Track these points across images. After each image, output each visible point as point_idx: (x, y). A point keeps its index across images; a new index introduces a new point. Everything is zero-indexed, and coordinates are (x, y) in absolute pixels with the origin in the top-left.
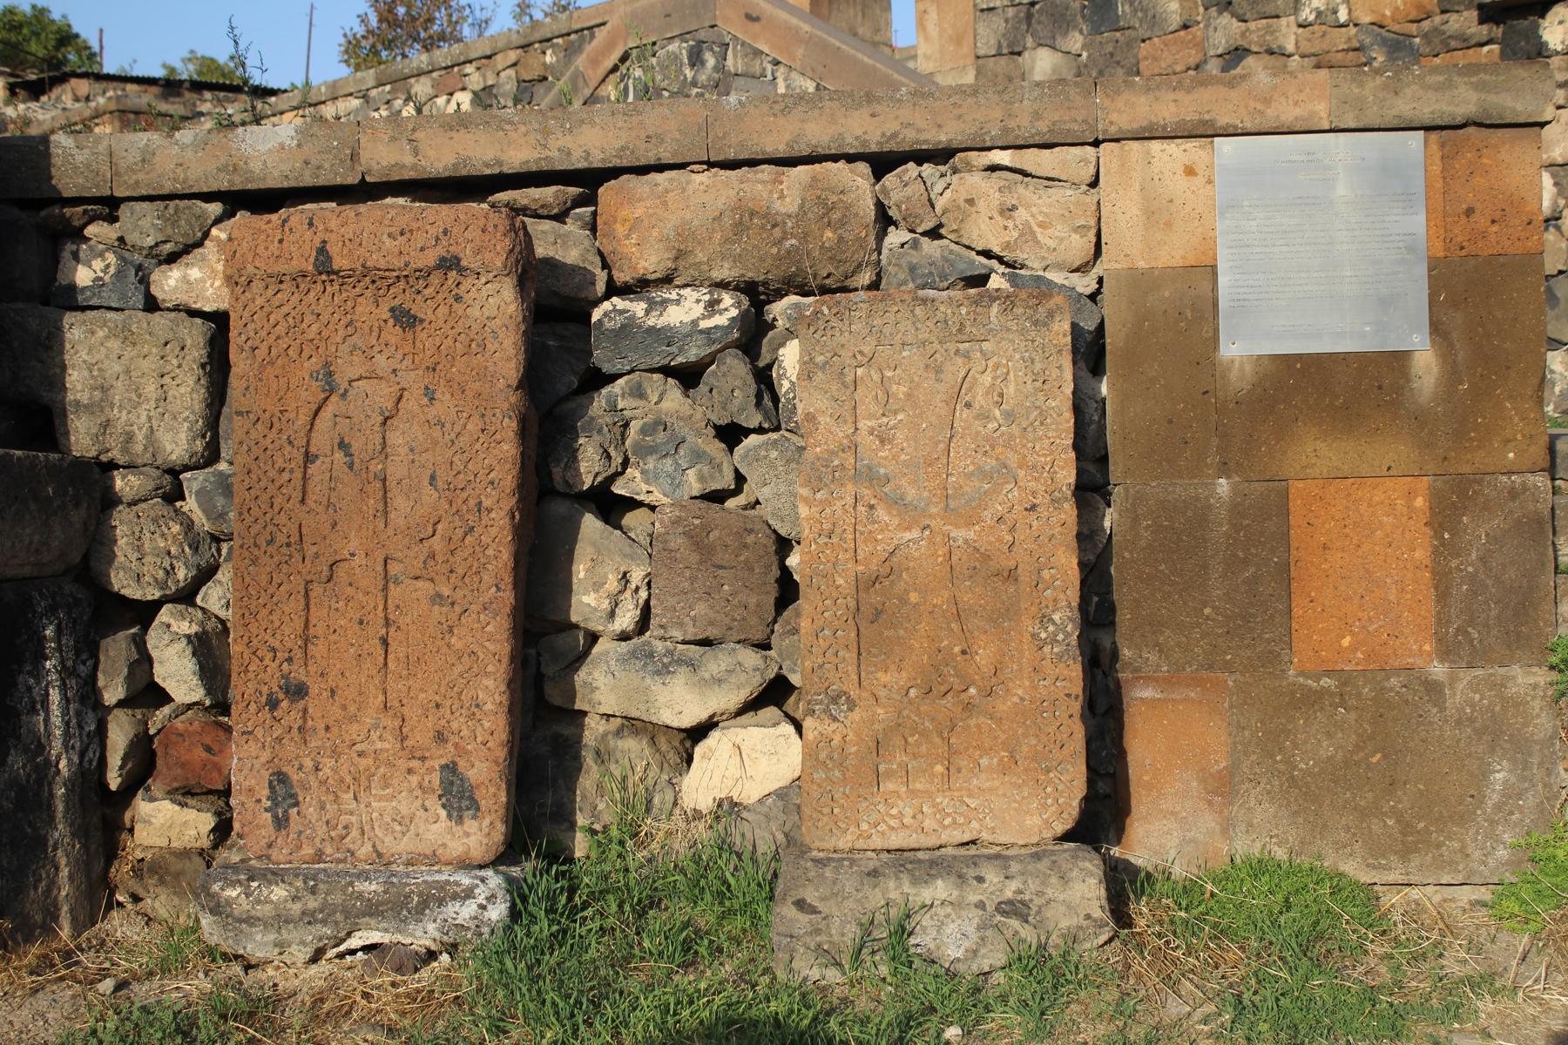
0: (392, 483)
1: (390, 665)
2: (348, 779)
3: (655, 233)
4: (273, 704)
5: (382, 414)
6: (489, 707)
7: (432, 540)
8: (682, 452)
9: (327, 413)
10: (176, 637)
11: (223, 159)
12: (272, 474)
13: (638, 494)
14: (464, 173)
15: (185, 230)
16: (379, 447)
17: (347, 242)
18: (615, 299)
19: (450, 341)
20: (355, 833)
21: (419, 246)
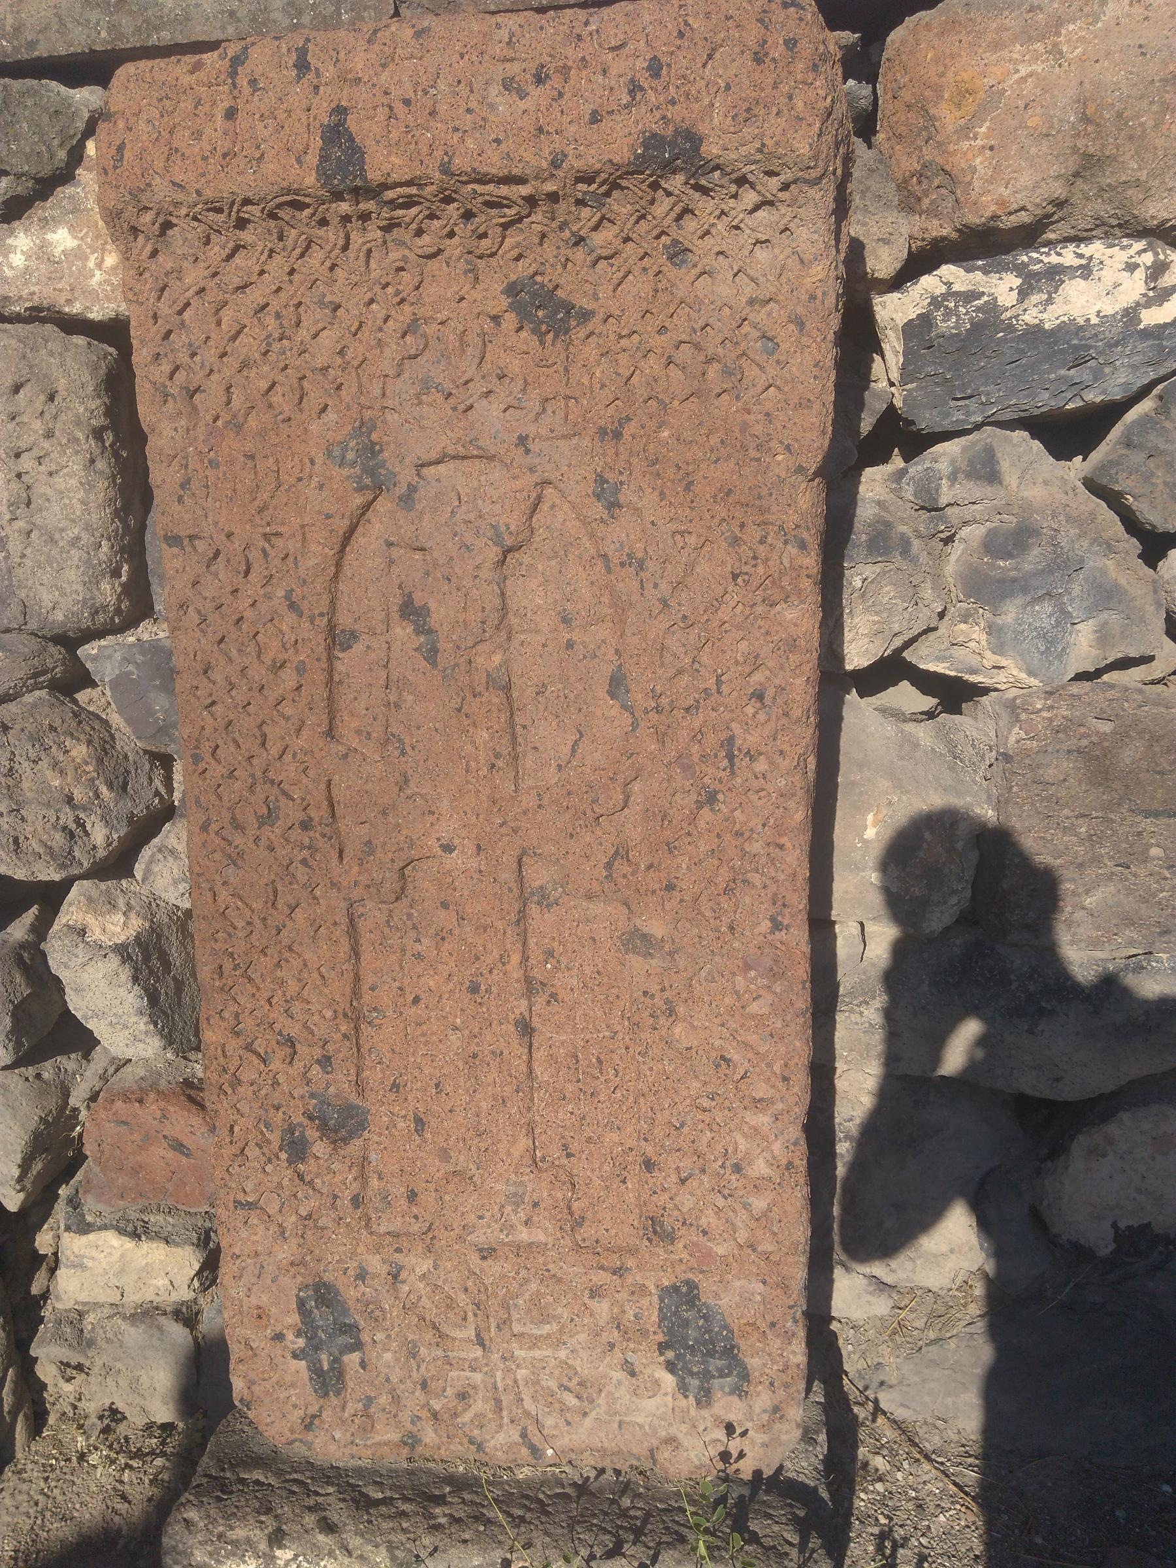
0: (523, 692)
1: (538, 1070)
2: (462, 1299)
4: (297, 1149)
5: (497, 539)
6: (760, 1168)
9: (370, 539)
12: (258, 673)
13: (974, 672)
16: (494, 618)
17: (399, 108)
19: (652, 365)
20: (479, 1405)
21: (587, 109)
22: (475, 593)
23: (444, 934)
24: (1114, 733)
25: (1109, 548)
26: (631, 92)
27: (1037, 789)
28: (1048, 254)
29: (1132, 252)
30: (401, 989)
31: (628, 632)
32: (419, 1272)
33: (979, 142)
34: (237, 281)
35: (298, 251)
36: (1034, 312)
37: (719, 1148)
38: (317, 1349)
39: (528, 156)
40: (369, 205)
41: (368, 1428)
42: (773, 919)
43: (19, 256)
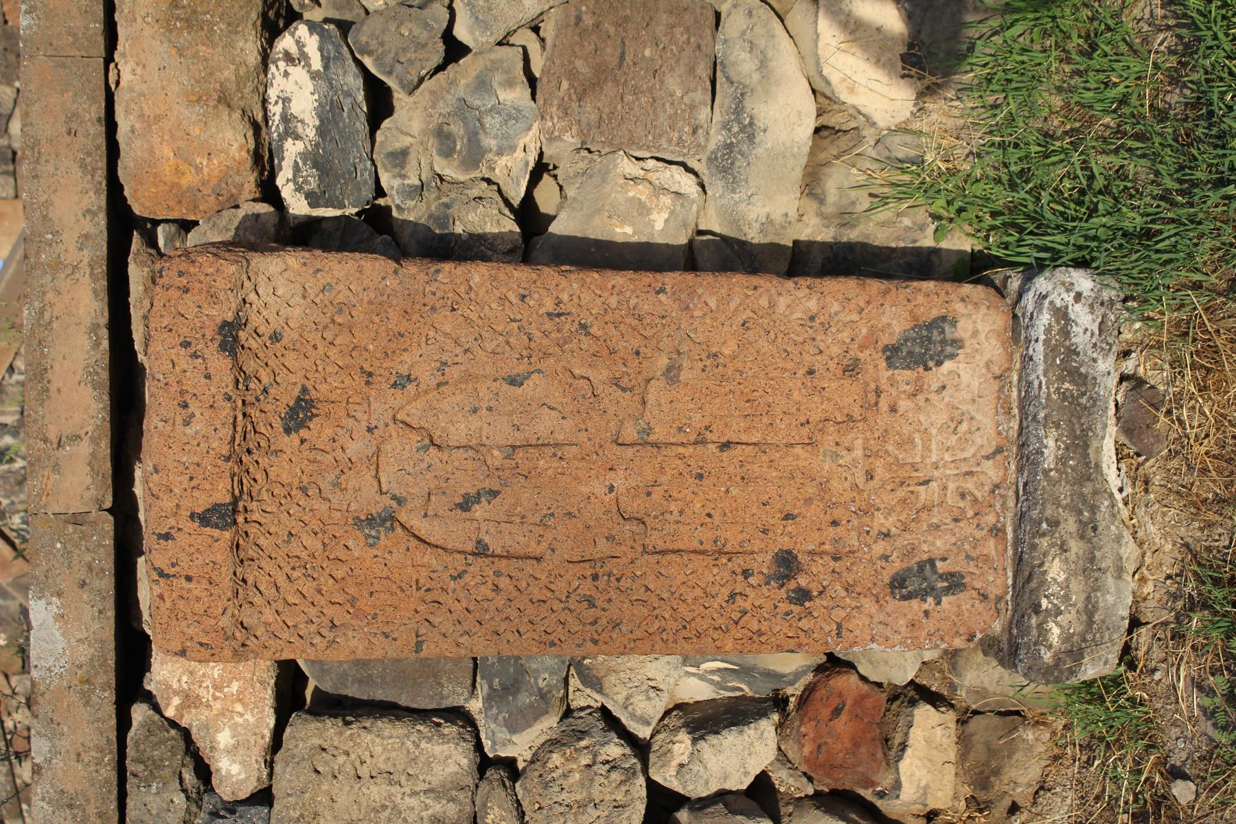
0: (518, 438)
1: (755, 440)
2: (901, 493)
3: (195, 131)
4: (802, 596)
6: (812, 305)
7: (595, 382)
8: (477, 103)
10: (695, 755)
11: (74, 697)
12: (500, 601)
13: (527, 164)
14: (105, 375)
15: (169, 754)
16: (471, 453)
17: (194, 483)
18: (280, 182)
19: (333, 353)
20: (969, 485)
21: (203, 380)
22: (456, 464)
23: (667, 495)
24: (569, 79)
25: (453, 83)
26: (197, 357)
27: (604, 126)
28: (273, 121)
29: (277, 73)
30: (702, 525)
31: (482, 373)
32: (883, 521)
33: (205, 163)
34: (274, 590)
35: (260, 551)
36: (308, 131)
37: (799, 329)
38: (933, 589)
39: (224, 413)
40: (241, 504)
41: (987, 559)
42: (658, 293)
43: (232, 768)
